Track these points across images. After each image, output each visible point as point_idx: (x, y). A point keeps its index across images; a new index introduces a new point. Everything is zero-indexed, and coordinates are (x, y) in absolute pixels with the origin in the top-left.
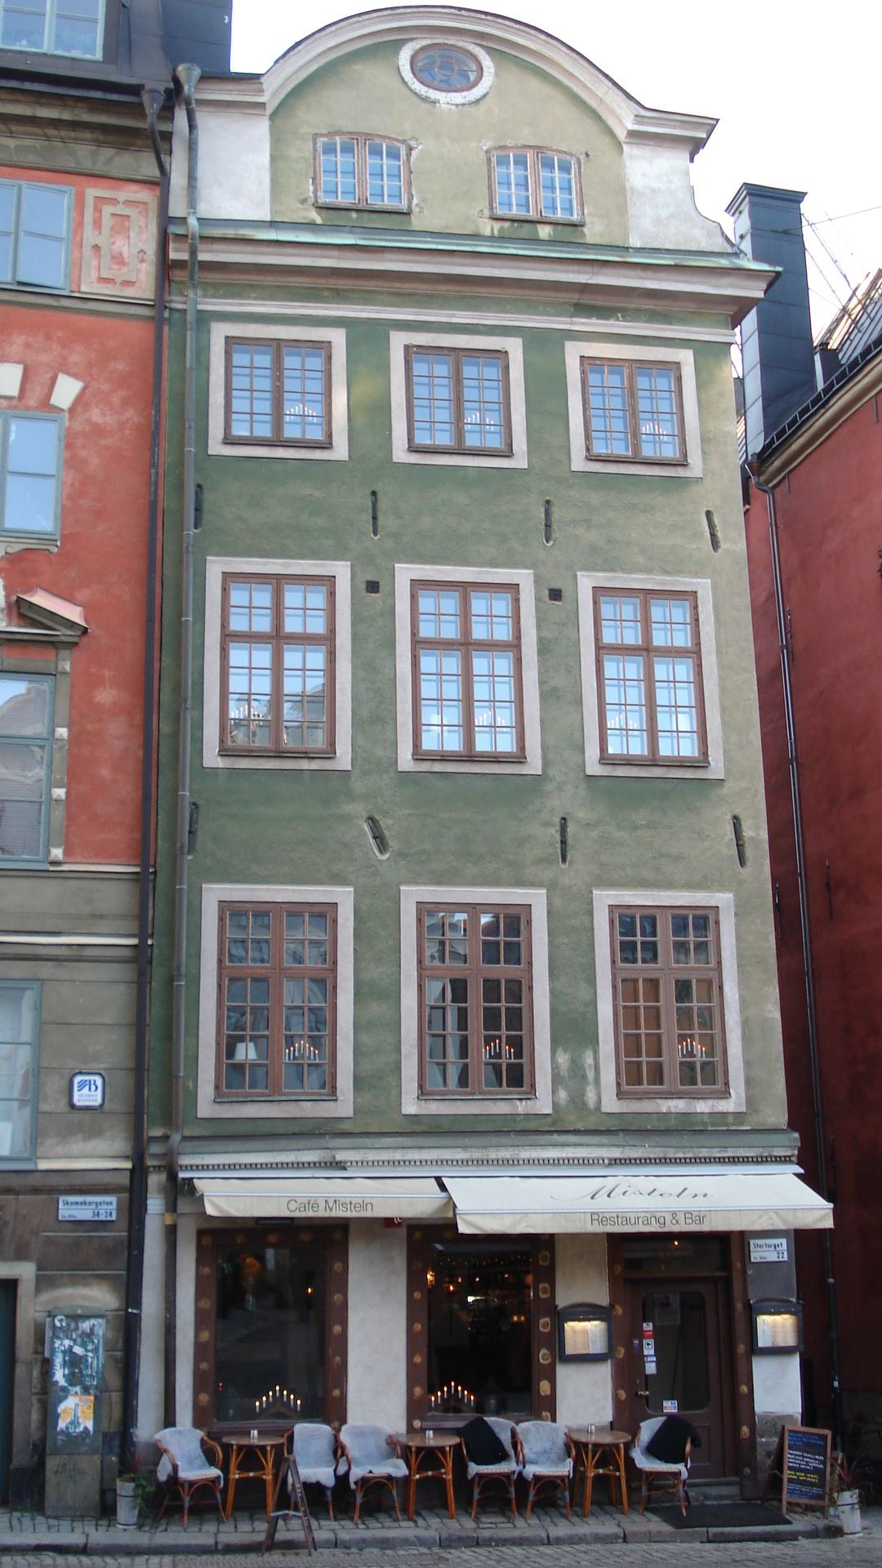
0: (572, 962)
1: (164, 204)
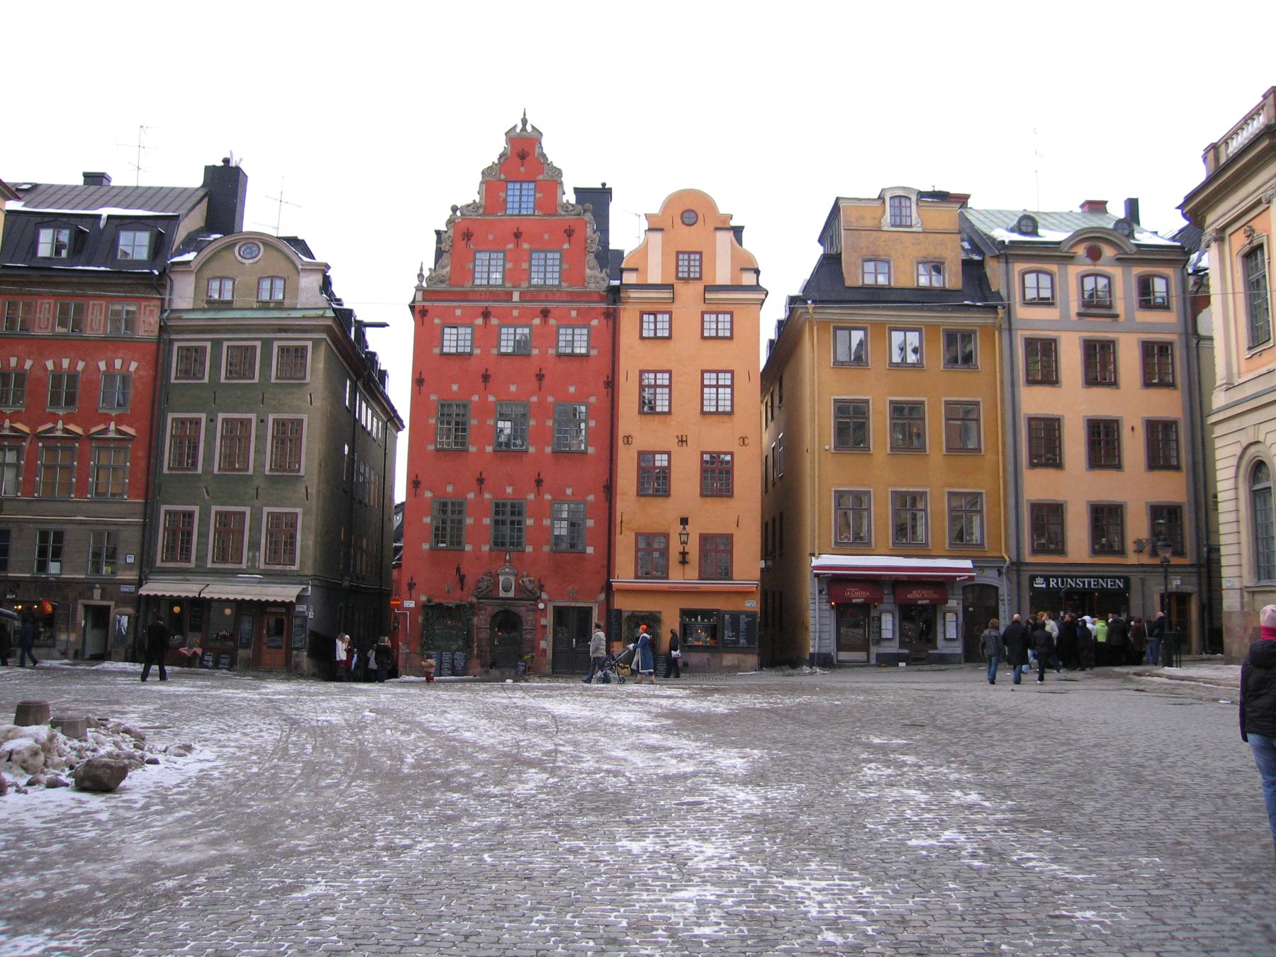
0: (255, 529)
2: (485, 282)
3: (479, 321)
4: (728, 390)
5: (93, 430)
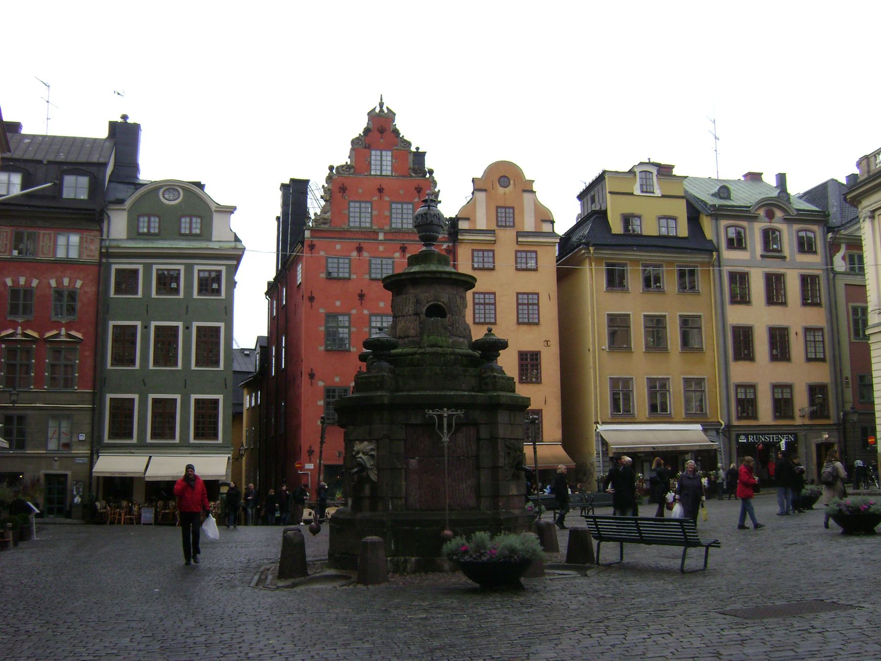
1: (102, 236)
2: (357, 224)
3: (354, 254)
4: (536, 307)
5: (48, 335)
